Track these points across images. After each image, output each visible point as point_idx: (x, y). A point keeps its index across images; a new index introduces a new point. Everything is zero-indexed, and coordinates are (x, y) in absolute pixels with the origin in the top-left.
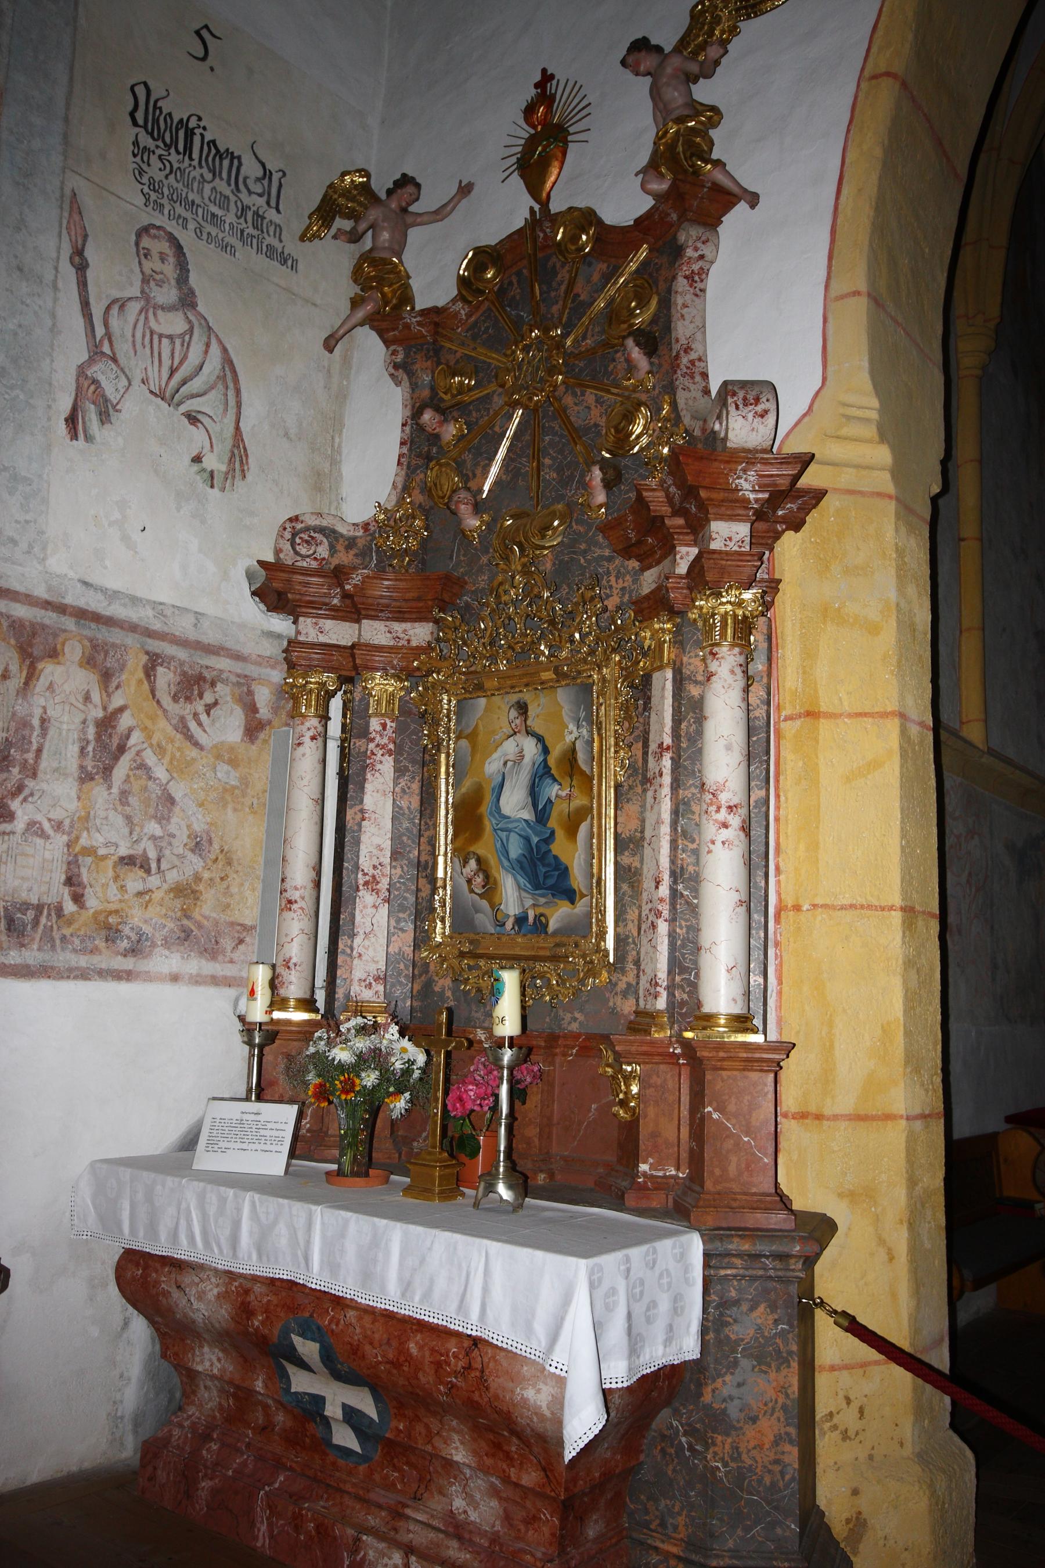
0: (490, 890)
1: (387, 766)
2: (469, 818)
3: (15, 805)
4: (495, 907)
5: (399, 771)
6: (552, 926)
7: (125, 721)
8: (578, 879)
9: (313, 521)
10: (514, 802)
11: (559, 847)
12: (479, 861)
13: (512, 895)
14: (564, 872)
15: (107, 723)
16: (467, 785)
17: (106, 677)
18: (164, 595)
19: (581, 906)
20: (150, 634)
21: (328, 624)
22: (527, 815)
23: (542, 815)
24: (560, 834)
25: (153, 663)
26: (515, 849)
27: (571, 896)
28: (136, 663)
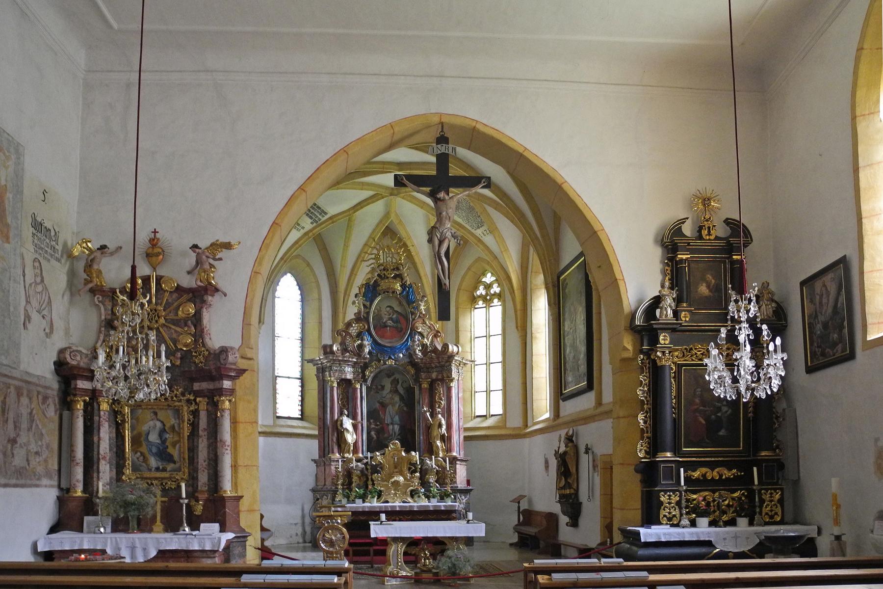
0: (145, 460)
1: (106, 425)
2: (136, 441)
3: (18, 439)
4: (148, 465)
5: (110, 426)
6: (168, 469)
7: (34, 412)
8: (176, 457)
9: (75, 348)
10: (154, 438)
11: (170, 450)
12: (141, 453)
13: (153, 462)
14: (171, 456)
15: (31, 413)
16: (135, 432)
17: (30, 399)
18: (38, 373)
19: (177, 465)
20: (37, 385)
21: (85, 382)
22: (159, 441)
23: (164, 442)
24: (170, 447)
25: (39, 393)
26: (154, 450)
27: (174, 462)
28: (35, 394)
